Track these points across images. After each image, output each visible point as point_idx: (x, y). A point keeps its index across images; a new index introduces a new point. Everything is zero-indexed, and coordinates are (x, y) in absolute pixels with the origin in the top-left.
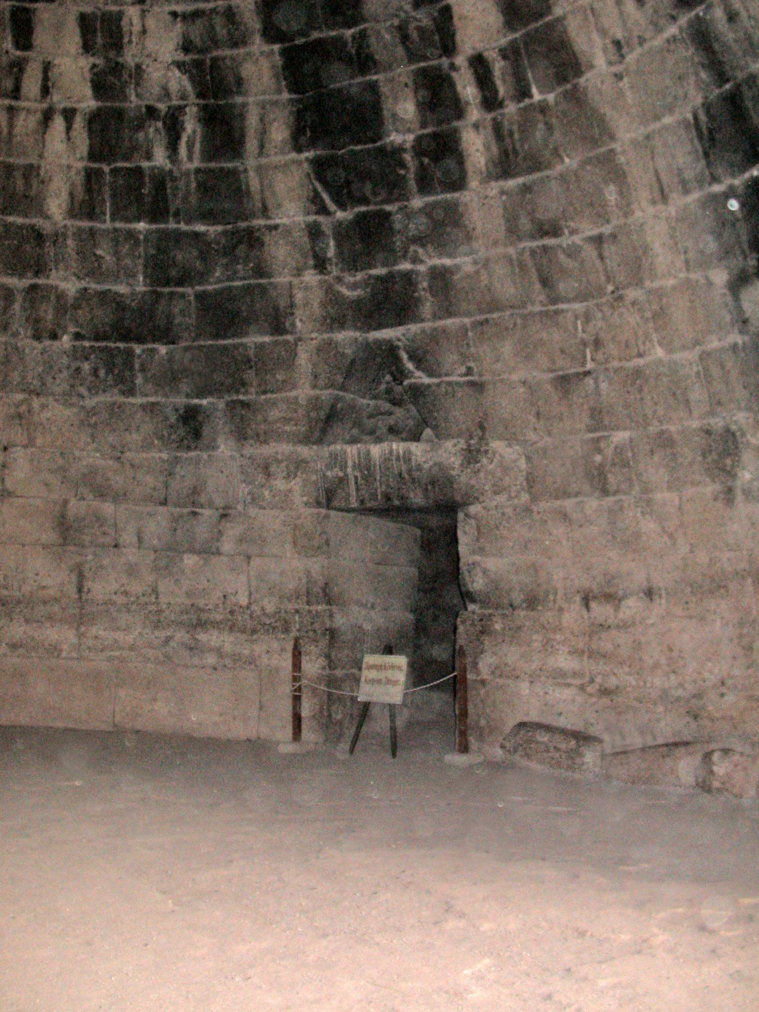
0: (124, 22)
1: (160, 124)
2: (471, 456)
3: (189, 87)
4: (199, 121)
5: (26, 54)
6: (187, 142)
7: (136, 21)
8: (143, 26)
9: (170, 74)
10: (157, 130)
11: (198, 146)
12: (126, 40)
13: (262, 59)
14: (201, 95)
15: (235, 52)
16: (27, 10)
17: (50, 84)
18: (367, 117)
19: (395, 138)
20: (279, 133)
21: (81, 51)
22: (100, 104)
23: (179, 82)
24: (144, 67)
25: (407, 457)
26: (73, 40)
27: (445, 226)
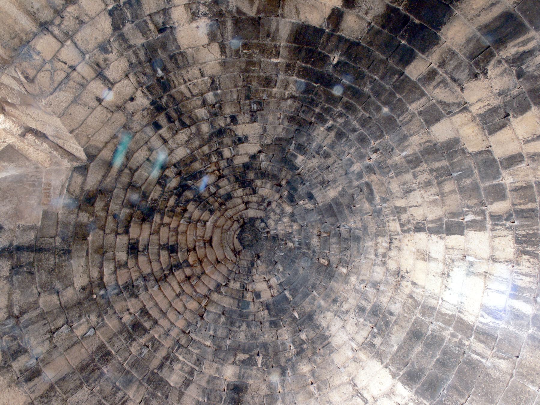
0: (481, 112)
1: (524, 67)
3: (492, 63)
4: (506, 47)
6: (524, 46)
7: (477, 106)
8: (477, 102)
9: (493, 76)
10: (527, 67)
11: (520, 40)
12: (490, 107)
13: (449, 37)
14: (492, 55)
15: (457, 51)
16: (501, 162)
17: (535, 137)
21: (508, 127)
22: (532, 105)
23: (493, 70)
24: (498, 91)
26: (504, 135)
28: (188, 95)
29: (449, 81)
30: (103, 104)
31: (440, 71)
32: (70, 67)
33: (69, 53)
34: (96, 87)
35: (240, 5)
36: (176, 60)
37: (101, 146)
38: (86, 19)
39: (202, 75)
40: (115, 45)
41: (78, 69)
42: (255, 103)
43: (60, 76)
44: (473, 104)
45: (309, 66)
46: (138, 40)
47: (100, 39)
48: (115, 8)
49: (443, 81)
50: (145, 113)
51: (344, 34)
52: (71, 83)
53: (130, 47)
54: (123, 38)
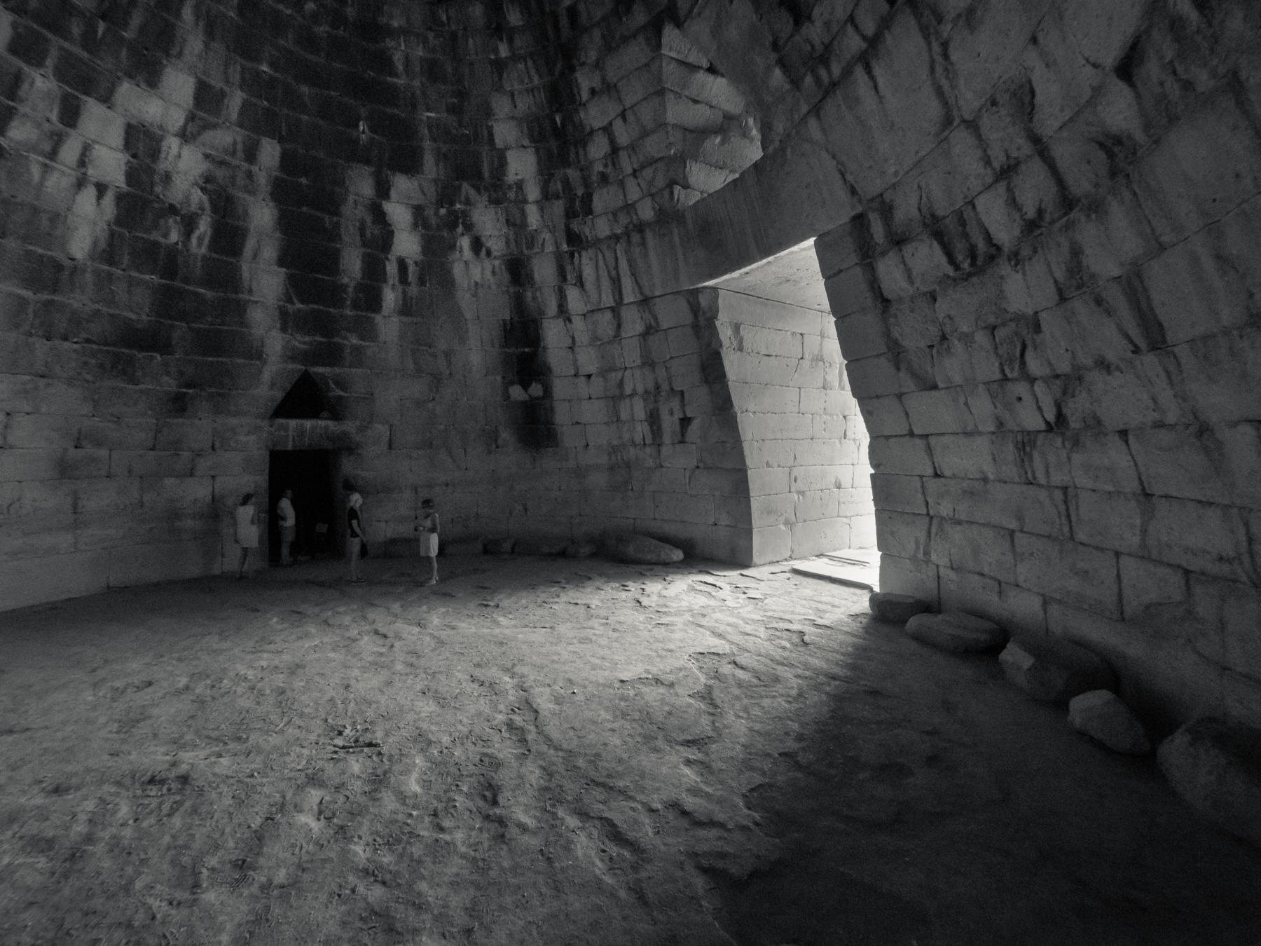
0: (164, 144)
2: (361, 429)
3: (207, 205)
5: (68, 130)
18: (331, 262)
19: (346, 280)
20: (270, 252)
23: (197, 196)
25: (326, 428)
27: (367, 331)
28: (530, 63)
29: (228, 158)
30: (619, 109)
31: (245, 165)
32: (636, 177)
33: (634, 193)
34: (623, 138)
35: (478, 198)
36: (540, 133)
37: (641, 39)
38: (611, 217)
39: (512, 95)
40: (594, 178)
41: (630, 171)
42: (443, 25)
43: (648, 173)
44: (180, 148)
45: (389, 110)
46: (573, 174)
47: (605, 191)
48: (587, 215)
49: (233, 153)
50: (583, 59)
51: (367, 170)
52: (642, 158)
53: (582, 170)
54: (586, 182)
